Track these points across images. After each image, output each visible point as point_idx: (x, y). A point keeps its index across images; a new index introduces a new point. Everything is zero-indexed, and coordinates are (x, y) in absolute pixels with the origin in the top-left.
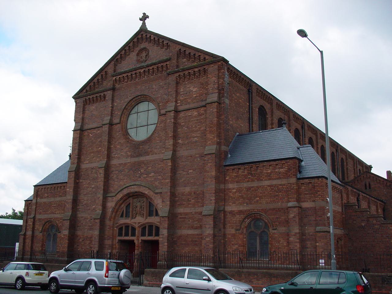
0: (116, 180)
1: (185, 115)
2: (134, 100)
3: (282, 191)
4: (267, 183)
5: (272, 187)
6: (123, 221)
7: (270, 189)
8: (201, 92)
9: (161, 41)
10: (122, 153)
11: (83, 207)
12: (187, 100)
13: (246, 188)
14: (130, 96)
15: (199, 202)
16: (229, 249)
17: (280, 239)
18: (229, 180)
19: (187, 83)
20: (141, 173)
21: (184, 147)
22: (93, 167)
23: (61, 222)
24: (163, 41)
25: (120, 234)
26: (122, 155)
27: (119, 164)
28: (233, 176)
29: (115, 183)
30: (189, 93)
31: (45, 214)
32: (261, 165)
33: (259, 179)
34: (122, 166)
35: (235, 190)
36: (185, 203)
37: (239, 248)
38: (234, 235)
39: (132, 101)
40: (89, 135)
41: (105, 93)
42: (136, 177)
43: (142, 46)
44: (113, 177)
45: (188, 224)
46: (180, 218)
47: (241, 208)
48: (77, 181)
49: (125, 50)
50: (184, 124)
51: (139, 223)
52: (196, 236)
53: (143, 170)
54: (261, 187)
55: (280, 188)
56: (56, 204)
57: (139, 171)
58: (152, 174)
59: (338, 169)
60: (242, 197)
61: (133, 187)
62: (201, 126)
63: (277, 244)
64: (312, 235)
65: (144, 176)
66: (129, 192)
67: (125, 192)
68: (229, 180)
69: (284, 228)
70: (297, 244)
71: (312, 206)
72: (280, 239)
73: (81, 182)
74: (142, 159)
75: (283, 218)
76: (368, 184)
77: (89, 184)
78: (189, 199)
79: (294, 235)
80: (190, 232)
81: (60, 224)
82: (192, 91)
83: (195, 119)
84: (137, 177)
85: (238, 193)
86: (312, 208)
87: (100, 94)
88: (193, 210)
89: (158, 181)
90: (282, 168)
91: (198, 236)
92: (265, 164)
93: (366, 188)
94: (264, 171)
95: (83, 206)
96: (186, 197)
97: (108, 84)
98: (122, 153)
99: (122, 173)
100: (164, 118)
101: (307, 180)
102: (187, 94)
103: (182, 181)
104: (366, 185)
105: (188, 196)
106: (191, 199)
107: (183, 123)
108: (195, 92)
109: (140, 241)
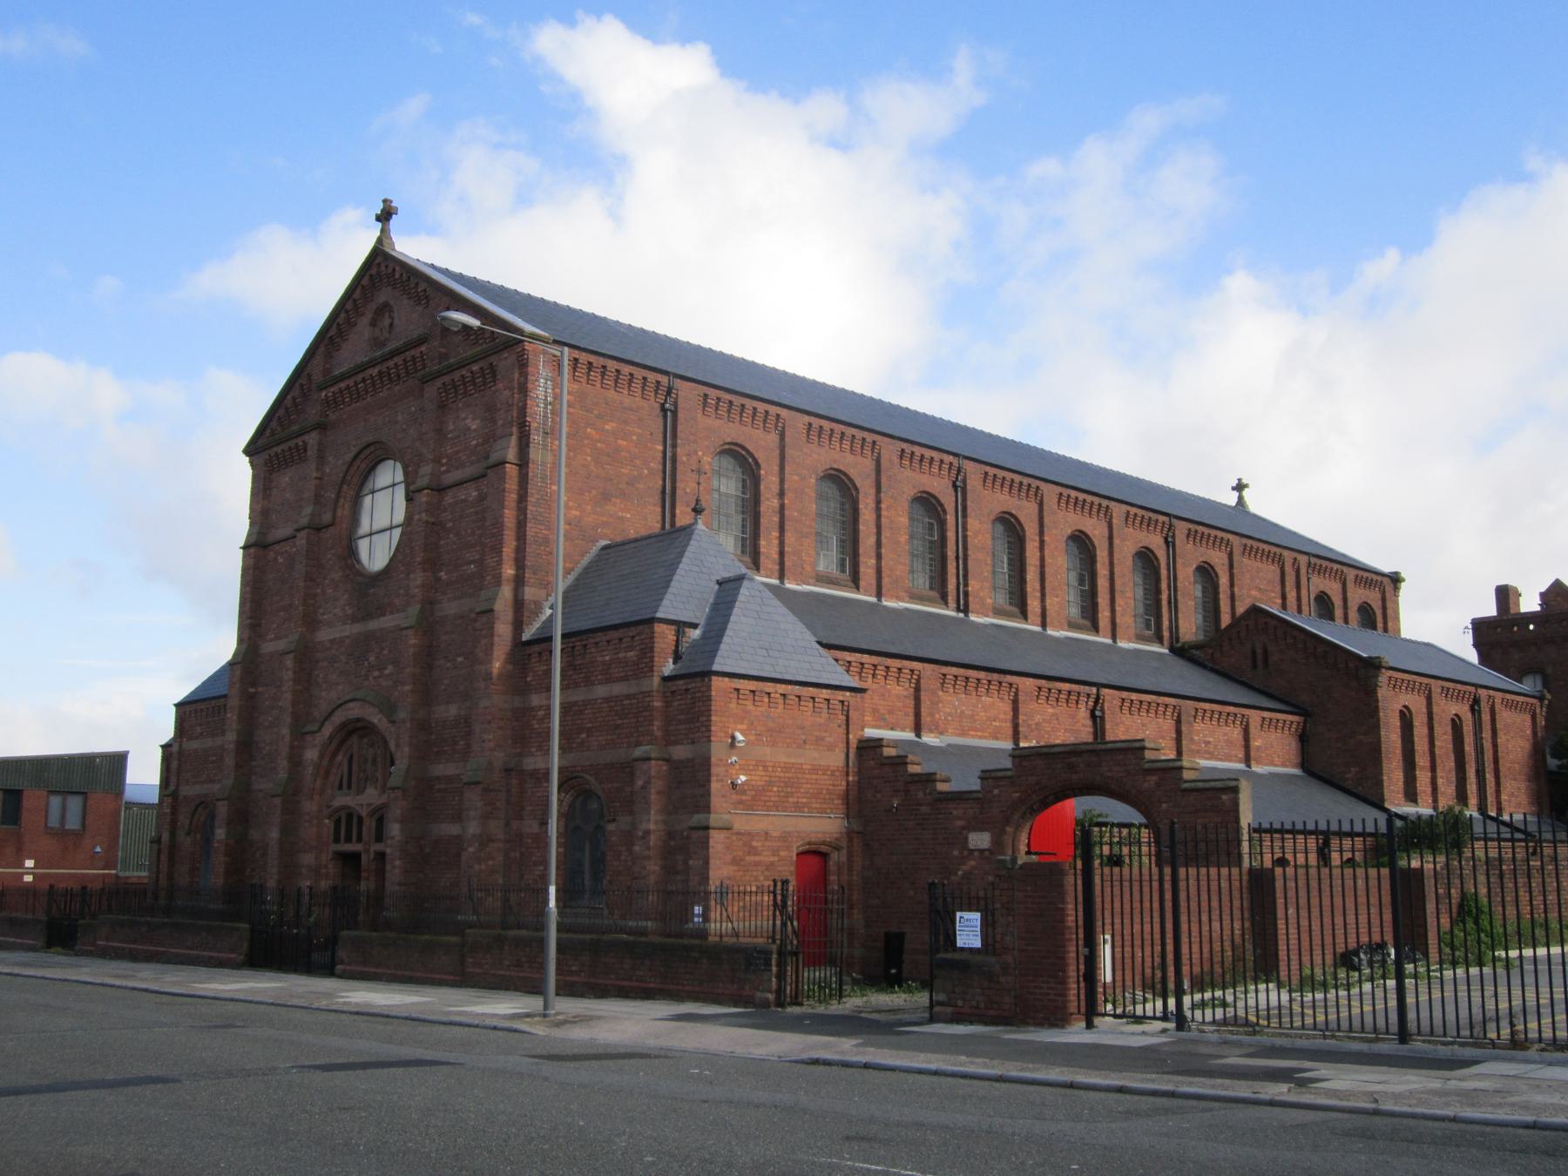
4: (601, 691)
6: (341, 800)
9: (413, 281)
24: (417, 284)
25: (337, 840)
26: (335, 615)
30: (465, 435)
32: (592, 641)
39: (358, 461)
40: (276, 559)
41: (306, 437)
46: (439, 791)
48: (252, 690)
51: (369, 805)
59: (1169, 602)
66: (343, 719)
67: (338, 718)
74: (374, 625)
76: (1259, 651)
87: (295, 441)
90: (631, 648)
92: (599, 637)
93: (1255, 666)
97: (313, 413)
101: (682, 682)
104: (1254, 653)
108: (475, 430)
109: (372, 856)
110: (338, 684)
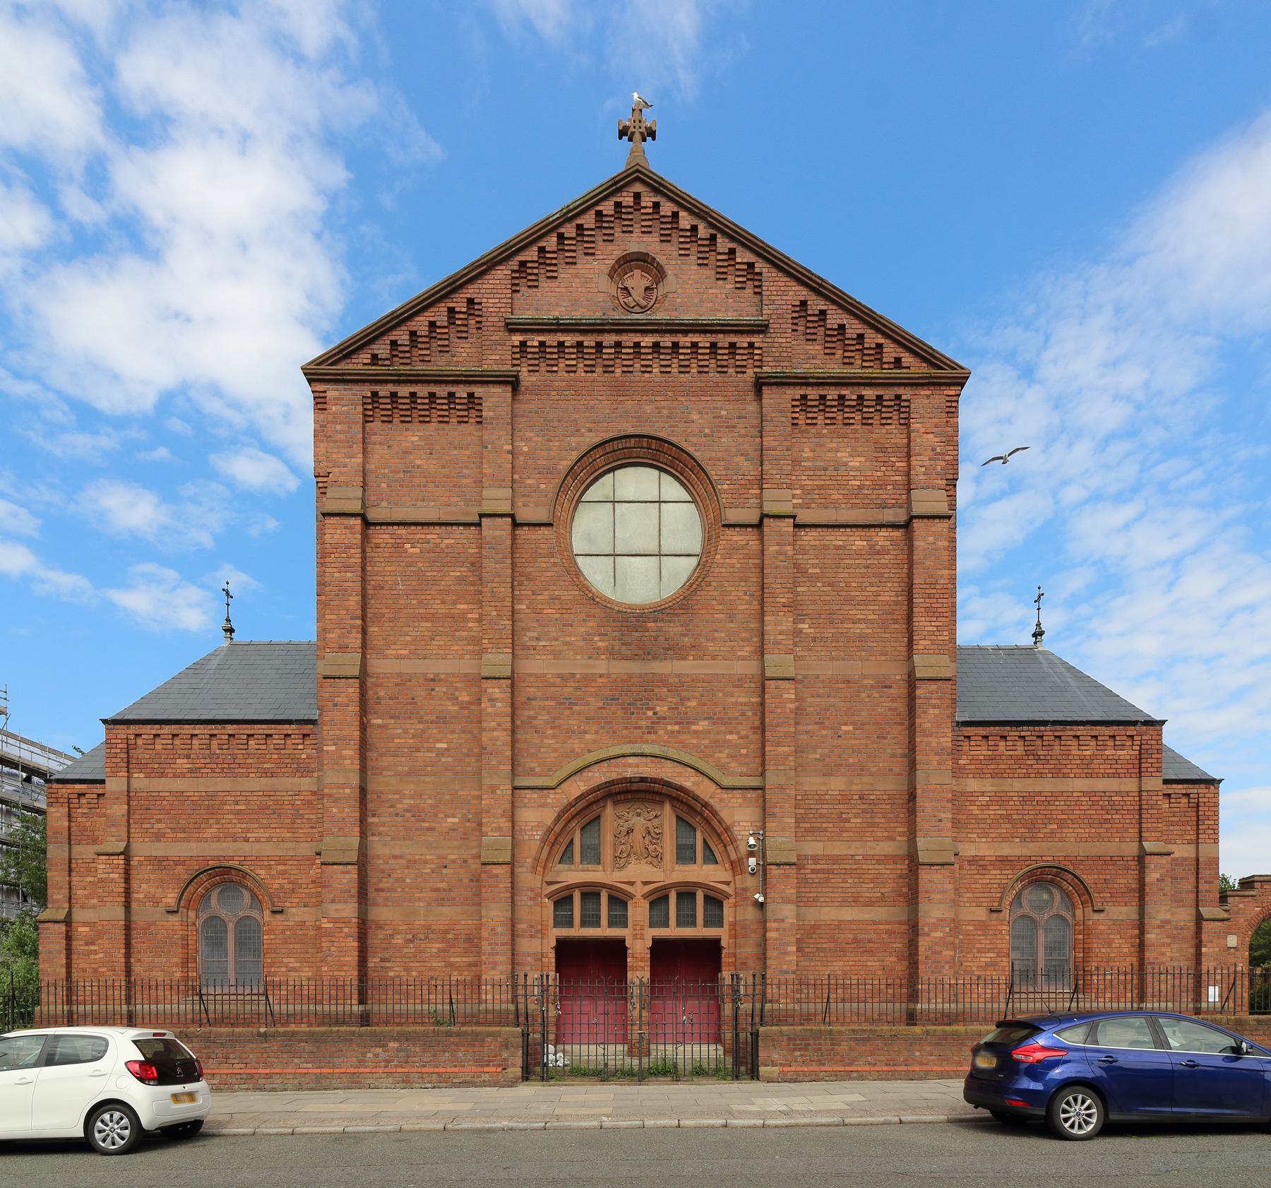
0: (549, 732)
1: (822, 543)
2: (608, 449)
3: (1122, 812)
4: (1080, 784)
5: (1093, 798)
6: (575, 874)
7: (1090, 803)
8: (879, 474)
10: (567, 639)
11: (400, 819)
12: (830, 492)
13: (1020, 794)
14: (590, 431)
15: (874, 825)
16: (968, 964)
17: (1111, 936)
18: (967, 767)
19: (825, 431)
20: (658, 718)
21: (820, 648)
22: (437, 675)
23: (283, 873)
26: (567, 644)
27: (563, 678)
28: (982, 758)
29: (546, 741)
31: (188, 840)
33: (1058, 773)
34: (572, 684)
35: (988, 799)
36: (831, 825)
37: (999, 959)
38: (982, 926)
42: (636, 728)
43: (636, 243)
44: (535, 718)
45: (840, 890)
46: (813, 872)
47: (1006, 850)
49: (561, 237)
50: (818, 571)
51: (645, 883)
52: (869, 927)
53: (665, 708)
54: (1065, 794)
55: (1117, 803)
56: (247, 802)
57: (648, 709)
58: (702, 725)
60: (1008, 818)
61: (631, 760)
62: (880, 589)
63: (1103, 950)
64: (1182, 929)
65: (669, 727)
66: (614, 776)
67: (599, 776)
68: (967, 767)
69: (1124, 909)
70: (1164, 949)
71: (1186, 855)
72: (1111, 936)
73: (380, 726)
75: (1121, 881)
77: (419, 736)
78: (844, 816)
79: (1159, 927)
80: (849, 914)
81: (280, 881)
82: (846, 464)
83: (857, 561)
84: (639, 728)
85: (997, 807)
86: (1185, 859)
87: (452, 389)
88: (856, 849)
89: (727, 751)
91: (875, 927)
94: (1073, 752)
95: (397, 815)
96: (831, 806)
98: (567, 639)
99: (576, 708)
100: (741, 538)
101: (1180, 786)
102: (828, 473)
103: (818, 756)
105: (840, 806)
106: (849, 816)
107: (814, 566)
110: (585, 732)
